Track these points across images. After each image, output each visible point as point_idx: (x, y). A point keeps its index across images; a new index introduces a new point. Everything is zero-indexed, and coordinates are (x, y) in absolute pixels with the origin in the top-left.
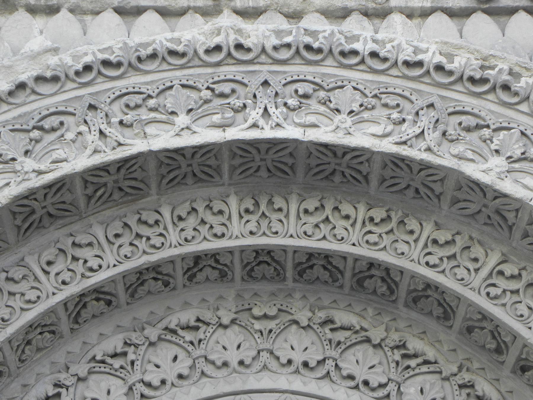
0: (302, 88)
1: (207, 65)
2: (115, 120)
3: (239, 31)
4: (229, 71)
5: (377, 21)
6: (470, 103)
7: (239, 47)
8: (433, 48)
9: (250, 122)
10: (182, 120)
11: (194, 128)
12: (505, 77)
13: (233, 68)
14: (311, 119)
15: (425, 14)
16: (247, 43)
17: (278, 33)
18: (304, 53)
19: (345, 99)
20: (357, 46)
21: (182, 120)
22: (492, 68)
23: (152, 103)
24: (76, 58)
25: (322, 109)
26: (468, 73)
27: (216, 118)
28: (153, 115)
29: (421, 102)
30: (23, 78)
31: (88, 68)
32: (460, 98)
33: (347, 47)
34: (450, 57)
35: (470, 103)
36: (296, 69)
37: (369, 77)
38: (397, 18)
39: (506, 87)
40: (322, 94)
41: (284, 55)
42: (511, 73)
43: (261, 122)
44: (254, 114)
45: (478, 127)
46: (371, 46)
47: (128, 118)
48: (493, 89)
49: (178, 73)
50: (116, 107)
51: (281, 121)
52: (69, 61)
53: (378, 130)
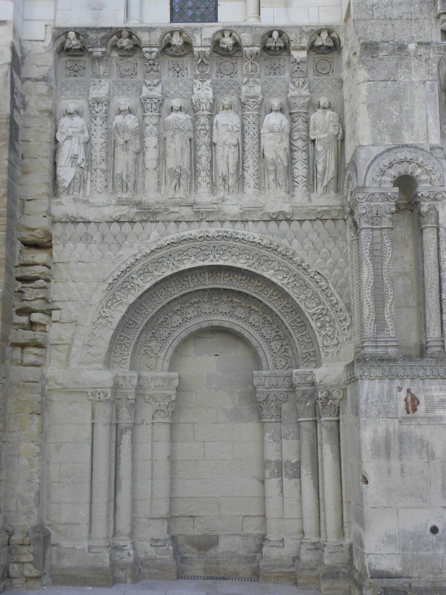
0: (224, 248)
1: (199, 241)
2: (176, 259)
3: (207, 232)
4: (205, 242)
5: (245, 223)
6: (267, 253)
7: (207, 236)
8: (258, 237)
9: (210, 259)
10: (193, 258)
11: (197, 261)
12: (276, 248)
13: (206, 242)
14: (226, 258)
15: (258, 221)
16: (210, 235)
17: (218, 232)
18: (225, 238)
19: (235, 251)
20: (238, 236)
21: (193, 258)
22: (273, 244)
23: (185, 253)
24: (165, 241)
25: (229, 254)
26: (267, 246)
27: (202, 258)
28: (186, 257)
29: (254, 253)
30: (152, 249)
31: (168, 244)
32: (264, 252)
33: (236, 237)
34: (262, 240)
35: (267, 253)
36: (222, 242)
37: (242, 244)
38: (250, 223)
39: (276, 250)
40: (229, 250)
41: (219, 238)
42: (277, 246)
43: (213, 260)
44: (212, 257)
45: (268, 260)
46: (242, 237)
47: (179, 258)
48: (273, 250)
49: (192, 244)
50: (176, 255)
51: (218, 259)
52: (163, 243)
53: (242, 261)
